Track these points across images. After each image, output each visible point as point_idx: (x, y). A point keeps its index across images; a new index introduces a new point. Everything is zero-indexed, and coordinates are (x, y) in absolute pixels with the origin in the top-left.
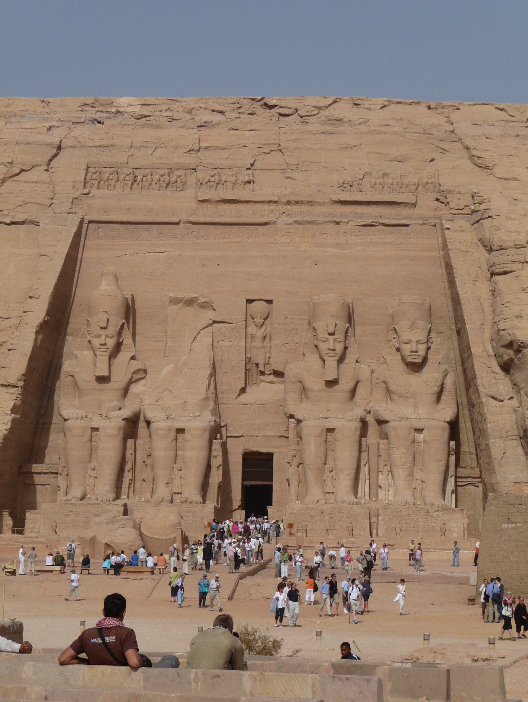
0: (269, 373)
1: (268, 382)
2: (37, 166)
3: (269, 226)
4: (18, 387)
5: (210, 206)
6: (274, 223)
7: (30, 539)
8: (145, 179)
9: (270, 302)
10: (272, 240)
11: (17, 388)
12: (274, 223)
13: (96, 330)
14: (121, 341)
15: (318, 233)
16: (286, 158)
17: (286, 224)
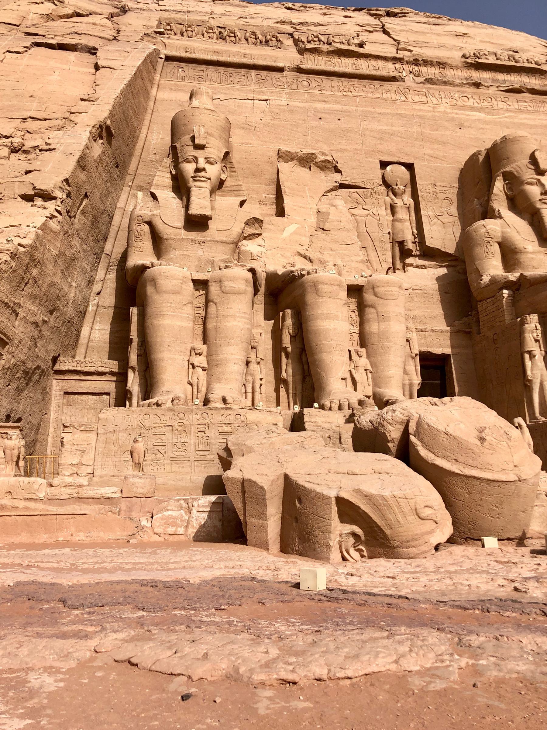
0: (418, 253)
1: (417, 267)
2: (96, 13)
3: (397, 83)
4: (55, 198)
5: (320, 58)
6: (403, 80)
7: (69, 490)
8: (232, 35)
9: (410, 167)
10: (403, 98)
11: (53, 201)
12: (403, 80)
13: (191, 152)
14: (223, 177)
15: (457, 95)
16: (394, 37)
17: (415, 82)
